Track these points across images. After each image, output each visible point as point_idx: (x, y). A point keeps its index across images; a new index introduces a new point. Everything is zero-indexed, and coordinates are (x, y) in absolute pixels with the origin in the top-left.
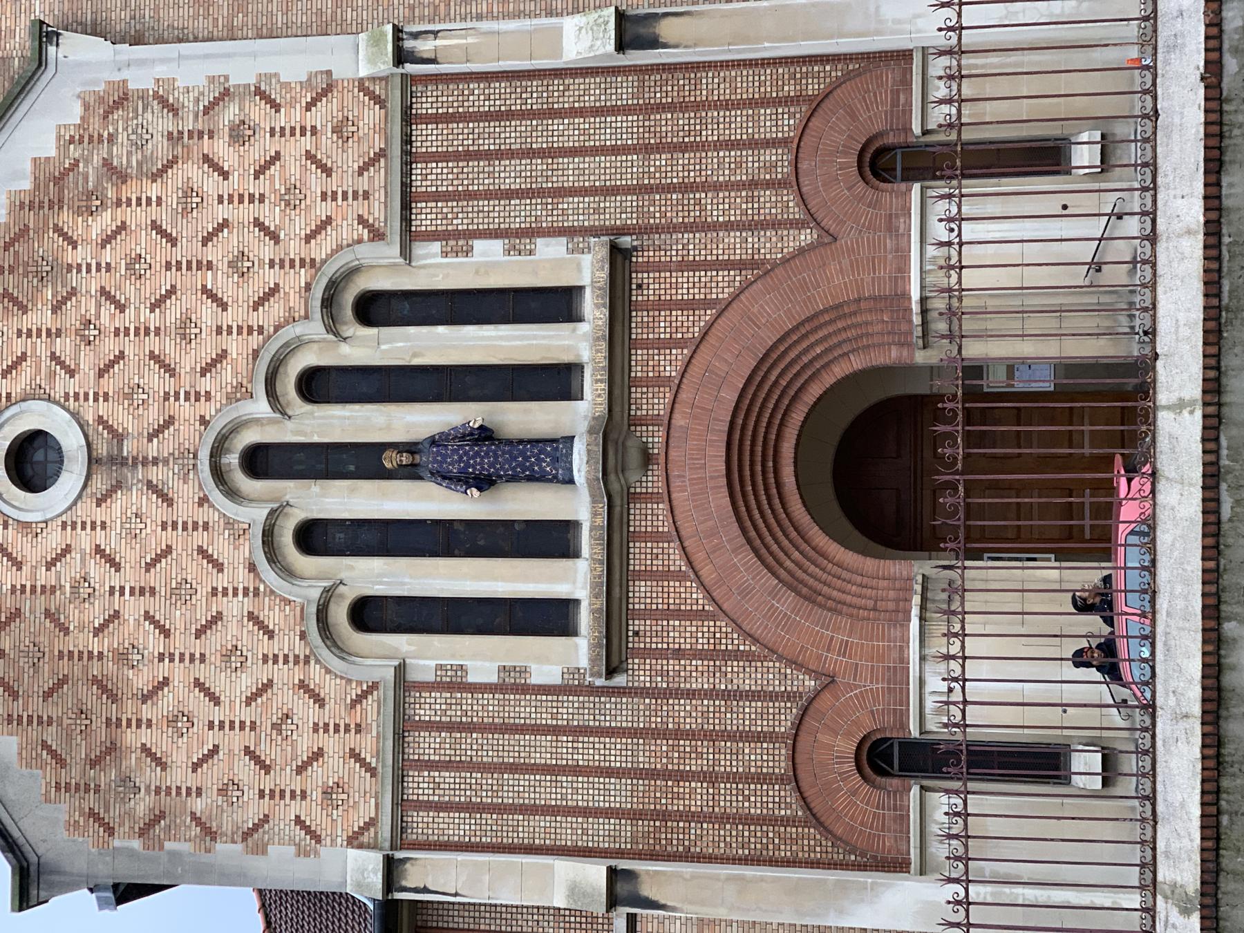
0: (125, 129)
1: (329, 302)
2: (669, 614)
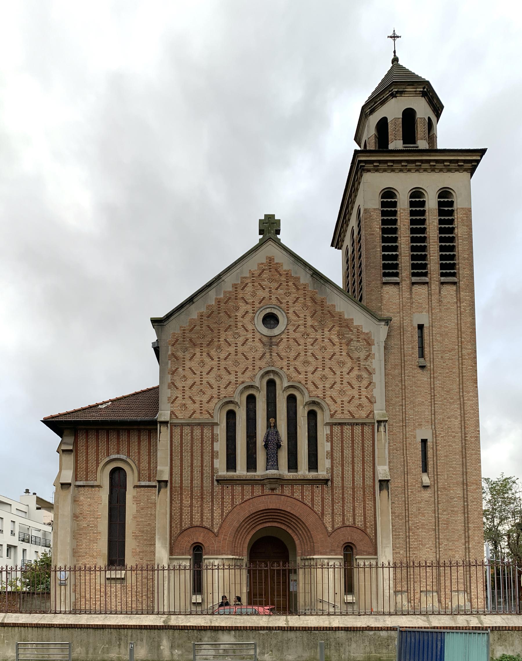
1: (314, 403)
2: (233, 495)
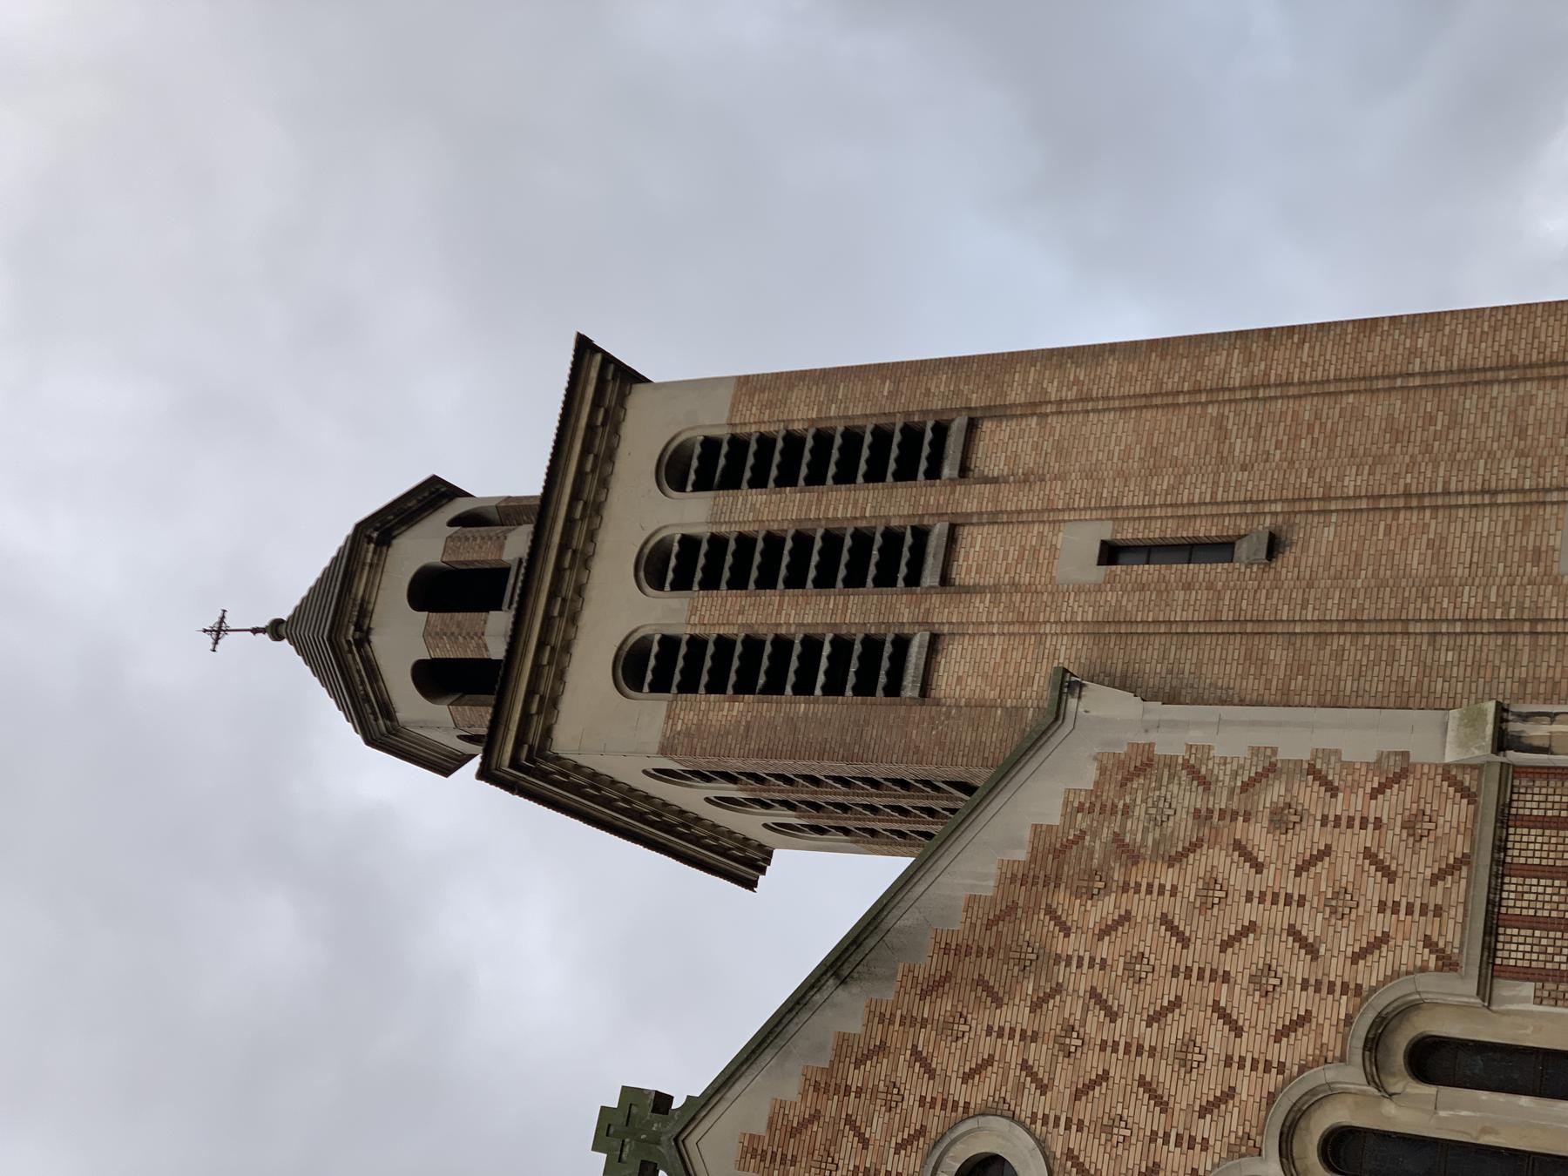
0: (1144, 801)
1: (1374, 1044)
